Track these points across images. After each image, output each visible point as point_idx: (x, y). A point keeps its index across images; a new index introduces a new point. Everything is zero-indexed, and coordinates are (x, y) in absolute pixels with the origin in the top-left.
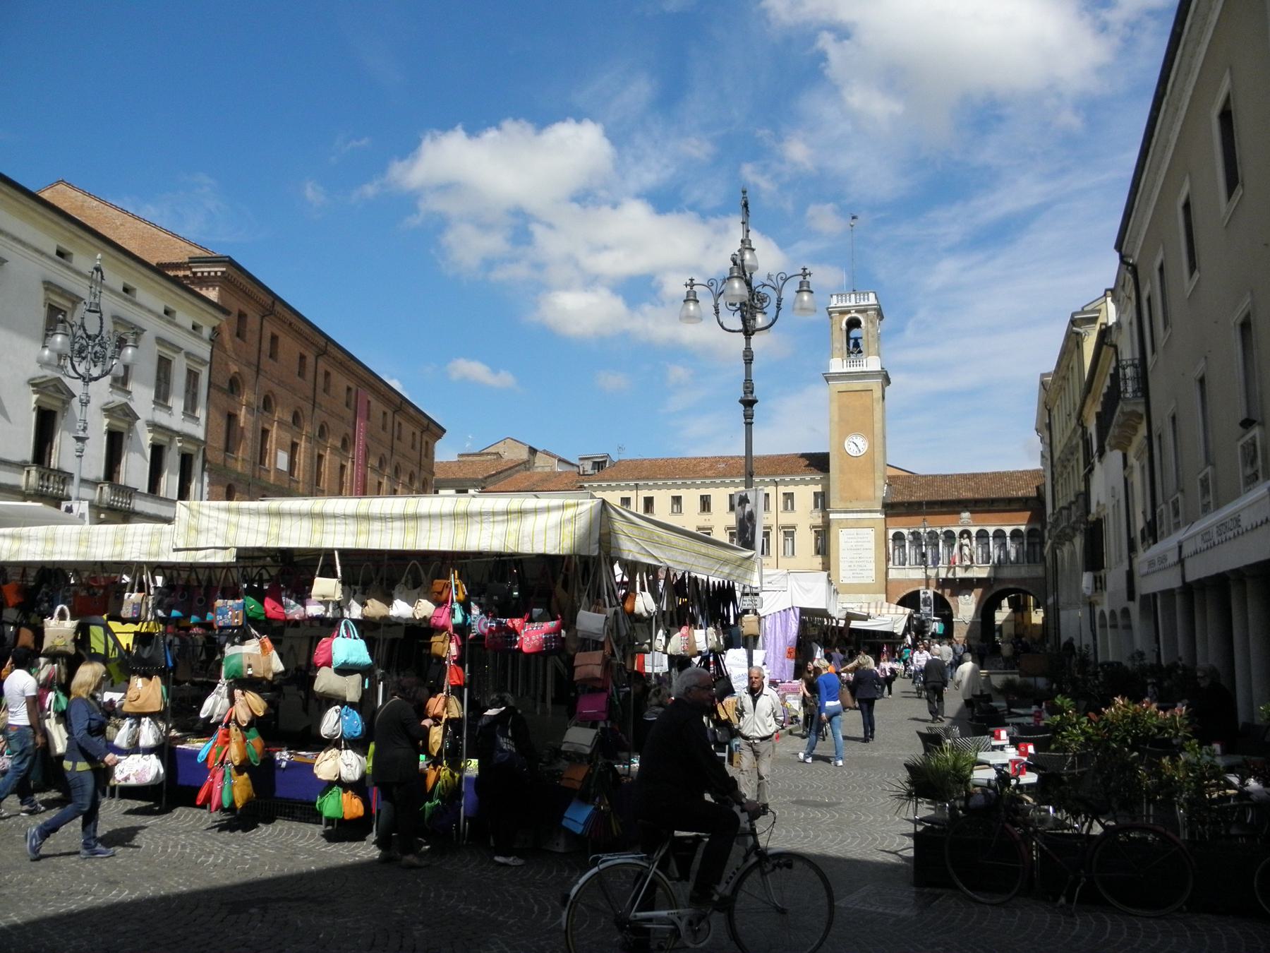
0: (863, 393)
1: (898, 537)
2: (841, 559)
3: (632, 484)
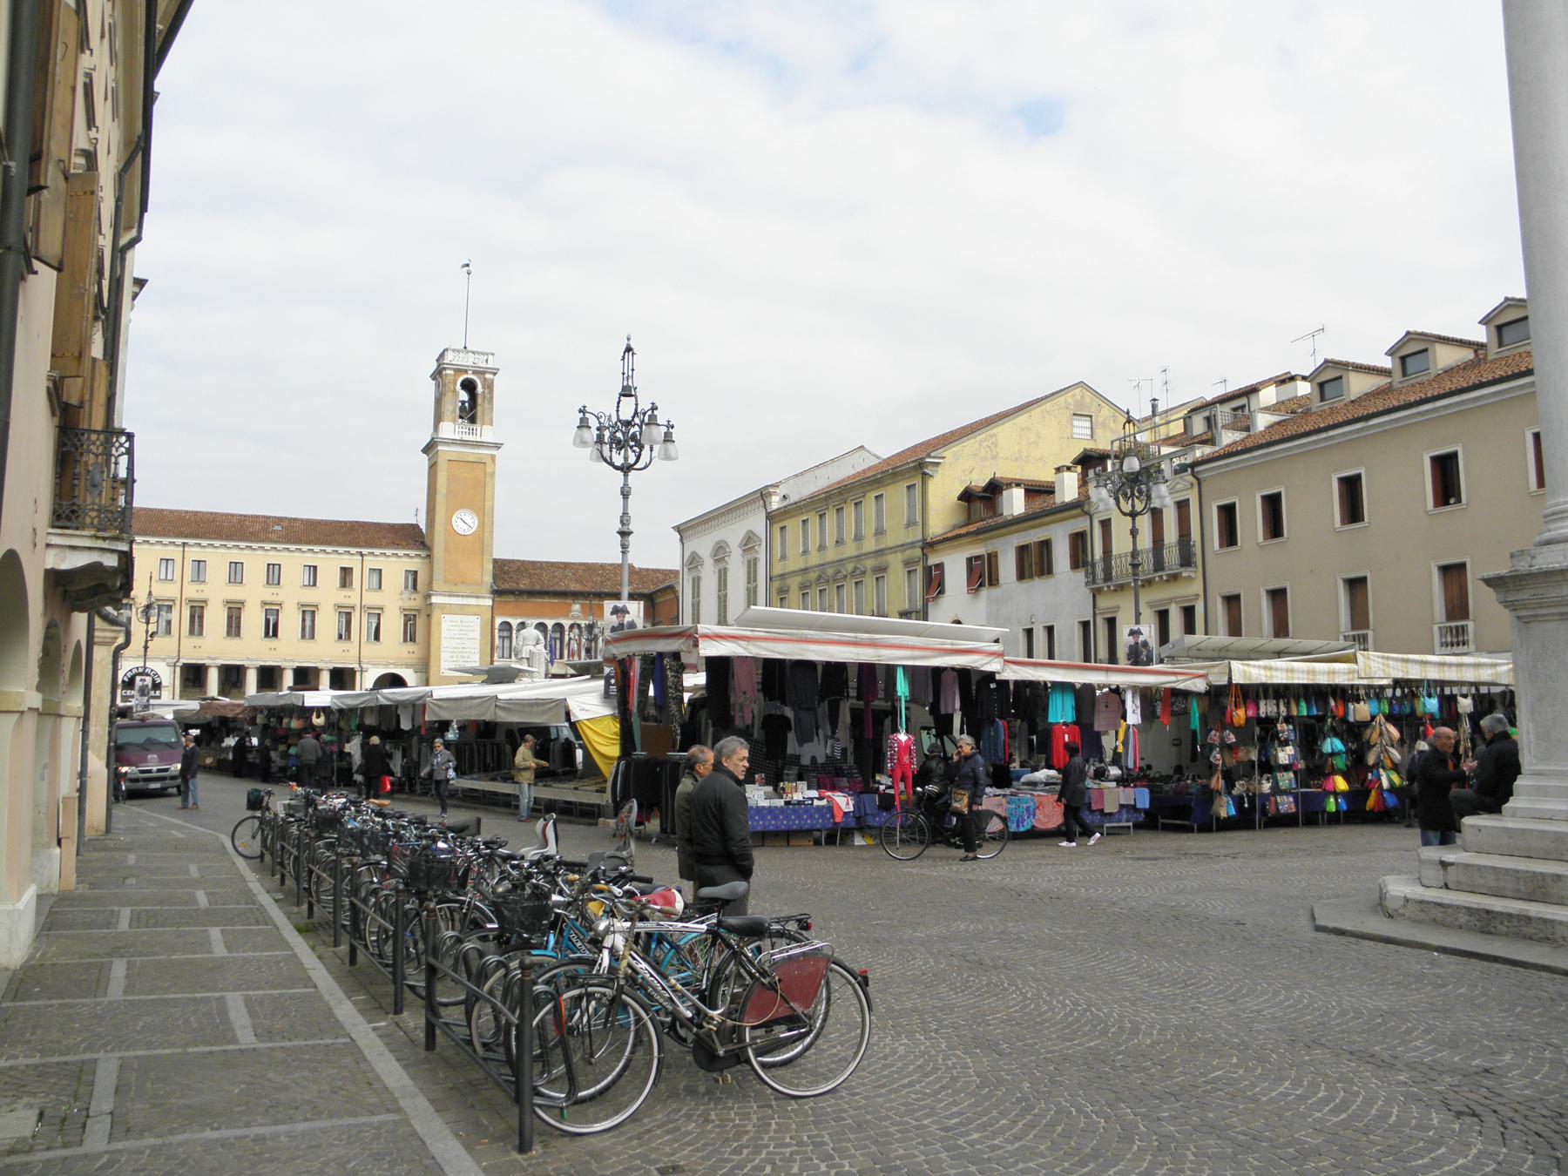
0: (475, 465)
1: (506, 626)
2: (442, 649)
3: (179, 541)
